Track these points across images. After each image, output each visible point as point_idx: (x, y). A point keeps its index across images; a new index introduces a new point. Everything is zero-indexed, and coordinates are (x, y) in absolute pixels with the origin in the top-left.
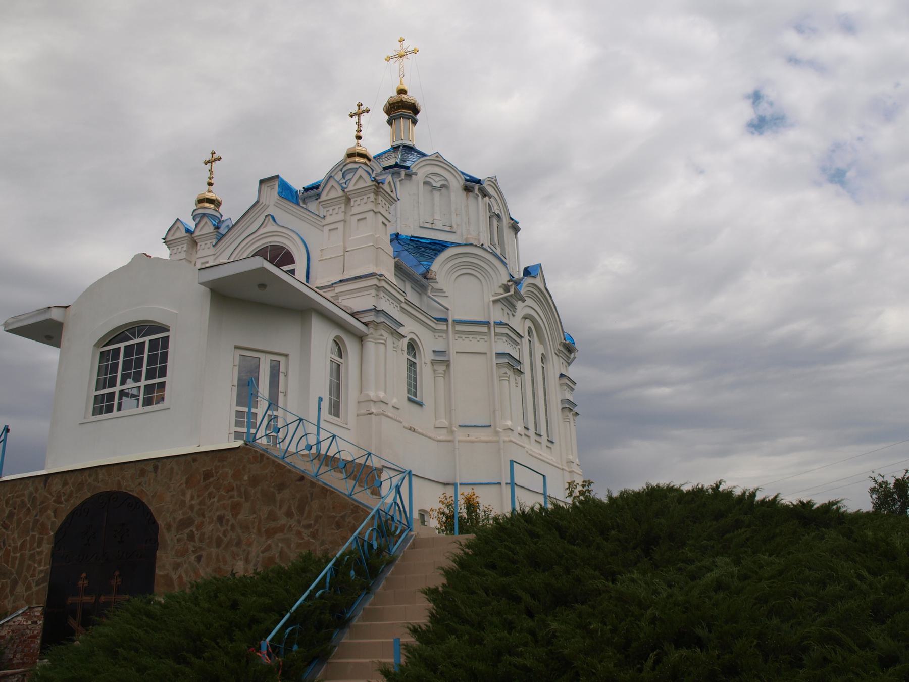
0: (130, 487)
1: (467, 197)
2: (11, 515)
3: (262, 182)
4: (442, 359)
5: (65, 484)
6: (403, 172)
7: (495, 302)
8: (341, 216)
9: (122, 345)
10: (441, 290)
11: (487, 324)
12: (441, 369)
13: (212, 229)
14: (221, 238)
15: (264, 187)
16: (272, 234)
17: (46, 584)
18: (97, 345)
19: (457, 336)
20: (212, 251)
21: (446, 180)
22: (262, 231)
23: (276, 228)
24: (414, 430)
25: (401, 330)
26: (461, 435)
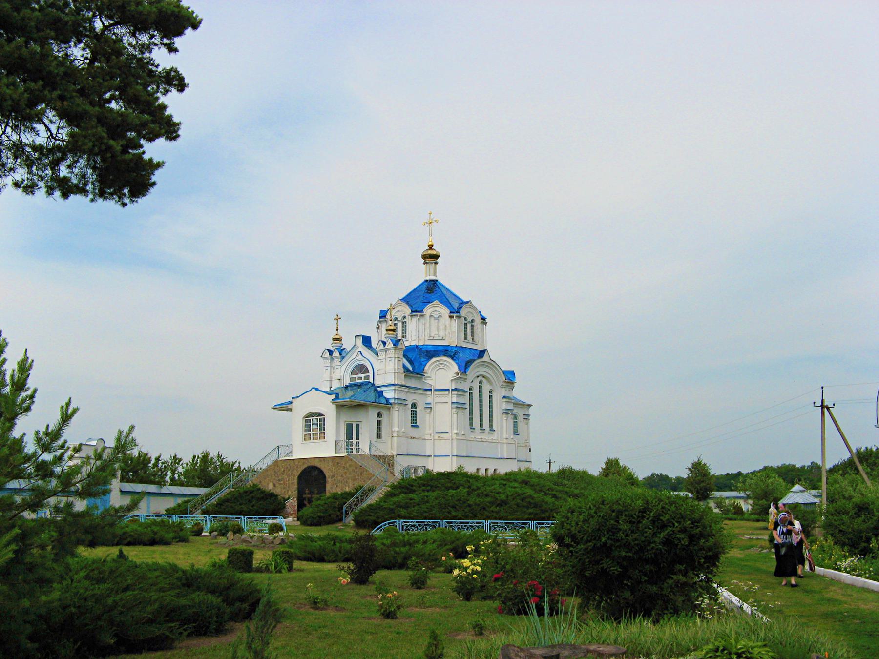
0: (317, 464)
1: (451, 321)
2: (284, 471)
3: (356, 336)
4: (429, 407)
5: (299, 462)
6: (419, 314)
7: (452, 380)
8: (384, 357)
9: (311, 418)
10: (430, 377)
11: (448, 390)
12: (428, 410)
13: (339, 355)
14: (343, 358)
15: (357, 338)
16: (361, 360)
17: (297, 491)
18: (304, 418)
19: (435, 396)
20: (339, 364)
21: (441, 313)
22: (357, 358)
23: (362, 357)
24: (414, 438)
25: (407, 403)
26: (436, 436)
